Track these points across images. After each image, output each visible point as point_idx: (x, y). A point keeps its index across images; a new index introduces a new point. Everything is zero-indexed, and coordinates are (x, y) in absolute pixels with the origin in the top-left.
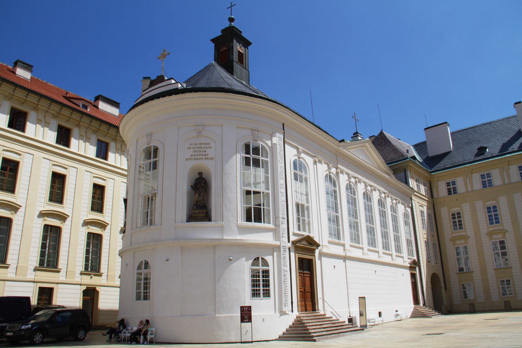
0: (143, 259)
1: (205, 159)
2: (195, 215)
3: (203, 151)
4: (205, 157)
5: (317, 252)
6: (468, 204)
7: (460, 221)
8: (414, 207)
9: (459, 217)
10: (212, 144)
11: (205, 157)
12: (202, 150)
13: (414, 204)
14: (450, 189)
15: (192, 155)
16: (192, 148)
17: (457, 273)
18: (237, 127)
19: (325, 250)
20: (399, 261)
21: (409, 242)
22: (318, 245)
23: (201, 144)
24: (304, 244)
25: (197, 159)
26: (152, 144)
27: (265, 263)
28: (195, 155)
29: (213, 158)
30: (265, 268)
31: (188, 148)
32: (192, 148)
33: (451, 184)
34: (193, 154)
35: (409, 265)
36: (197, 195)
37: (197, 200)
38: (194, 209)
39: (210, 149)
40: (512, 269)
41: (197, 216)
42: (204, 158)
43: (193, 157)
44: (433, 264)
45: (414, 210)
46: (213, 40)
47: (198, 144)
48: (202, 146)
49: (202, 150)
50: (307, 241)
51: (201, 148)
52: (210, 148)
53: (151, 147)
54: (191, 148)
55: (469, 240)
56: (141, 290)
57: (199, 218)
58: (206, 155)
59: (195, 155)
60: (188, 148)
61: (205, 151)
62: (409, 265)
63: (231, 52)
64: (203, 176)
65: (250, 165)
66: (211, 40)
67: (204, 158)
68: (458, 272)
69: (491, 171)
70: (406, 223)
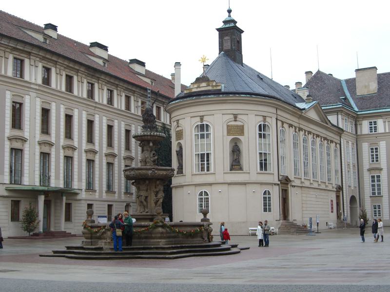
0: (203, 191)
5: (289, 184)
6: (385, 142)
7: (377, 155)
8: (342, 144)
9: (376, 152)
13: (342, 142)
14: (372, 127)
17: (370, 197)
19: (293, 184)
20: (330, 188)
21: (336, 171)
22: (290, 181)
24: (284, 181)
27: (269, 193)
30: (269, 196)
33: (373, 123)
35: (336, 190)
36: (235, 156)
44: (353, 188)
45: (342, 146)
46: (218, 30)
50: (286, 179)
55: (382, 172)
62: (336, 190)
65: (261, 138)
66: (218, 30)
68: (372, 195)
70: (336, 156)
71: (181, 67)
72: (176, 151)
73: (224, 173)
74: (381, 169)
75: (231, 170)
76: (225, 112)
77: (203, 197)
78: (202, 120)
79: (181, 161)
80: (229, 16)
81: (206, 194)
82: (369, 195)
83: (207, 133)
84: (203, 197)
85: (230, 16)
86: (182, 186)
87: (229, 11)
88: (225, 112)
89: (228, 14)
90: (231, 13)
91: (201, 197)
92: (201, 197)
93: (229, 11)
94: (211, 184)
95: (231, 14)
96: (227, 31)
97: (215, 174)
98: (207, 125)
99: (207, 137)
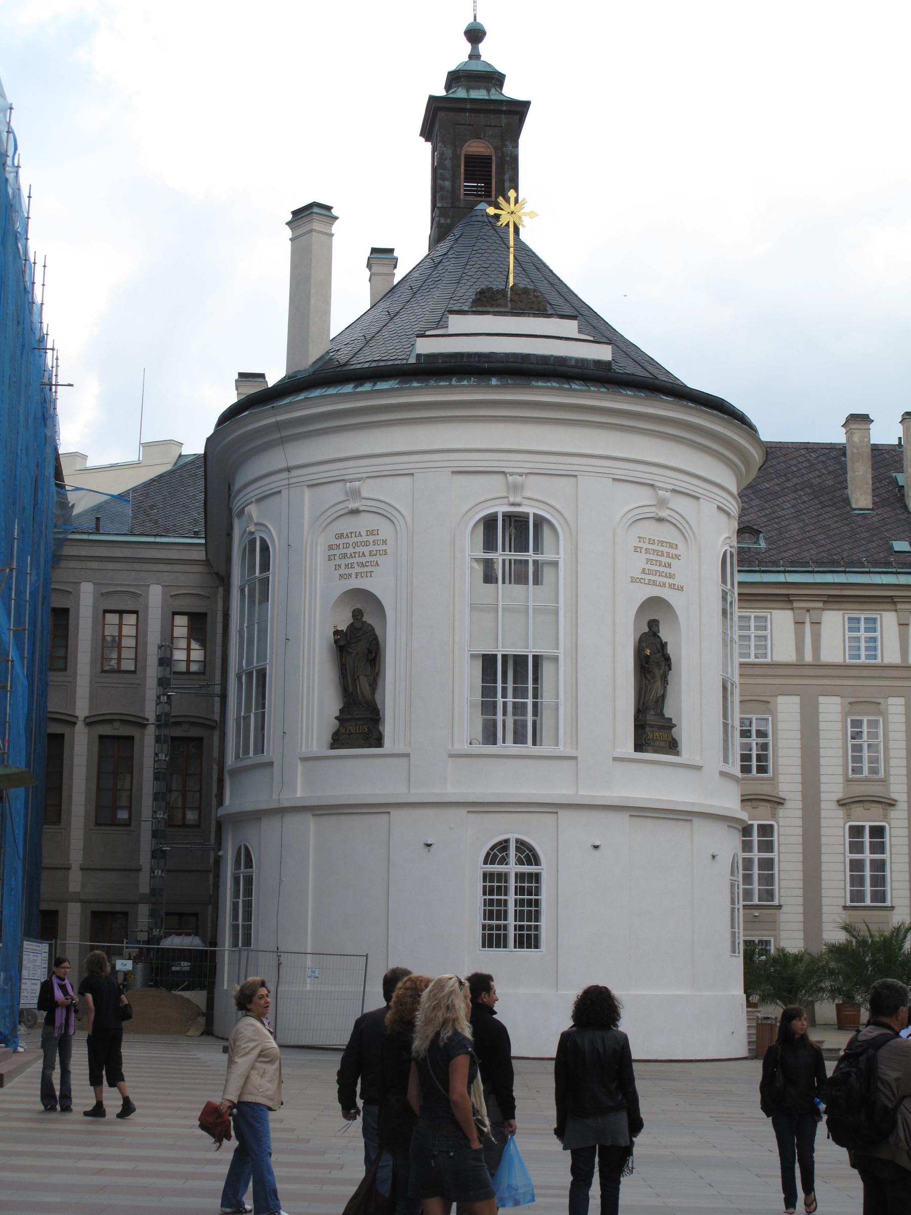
0: (513, 837)
1: (670, 585)
2: (653, 736)
3: (665, 564)
4: (671, 581)
10: (682, 550)
11: (671, 581)
12: (664, 560)
15: (643, 571)
16: (643, 551)
18: (719, 508)
23: (661, 543)
25: (654, 583)
26: (530, 509)
28: (650, 572)
29: (681, 589)
31: (636, 549)
32: (643, 551)
34: (648, 567)
37: (658, 696)
38: (651, 718)
39: (677, 560)
40: (781, 911)
41: (656, 737)
42: (667, 585)
43: (648, 577)
47: (656, 542)
48: (665, 550)
49: (664, 560)
51: (662, 555)
52: (677, 557)
53: (528, 514)
54: (641, 548)
56: (505, 919)
57: (662, 744)
58: (671, 576)
59: (650, 572)
60: (636, 549)
61: (670, 565)
63: (507, 176)
64: (664, 634)
67: (667, 585)
69: (771, 613)
71: (336, 228)
72: (336, 633)
73: (615, 759)
74: (779, 802)
75: (639, 747)
76: (622, 469)
77: (512, 868)
78: (516, 488)
79: (364, 683)
80: (470, 57)
81: (528, 854)
82: (843, 904)
83: (537, 557)
84: (512, 868)
85: (474, 56)
86: (382, 808)
87: (475, 35)
88: (622, 469)
89: (467, 47)
90: (481, 46)
91: (496, 868)
92: (496, 868)
93: (475, 35)
94: (553, 807)
95: (482, 47)
96: (482, 119)
97: (575, 758)
98: (540, 521)
99: (536, 582)
